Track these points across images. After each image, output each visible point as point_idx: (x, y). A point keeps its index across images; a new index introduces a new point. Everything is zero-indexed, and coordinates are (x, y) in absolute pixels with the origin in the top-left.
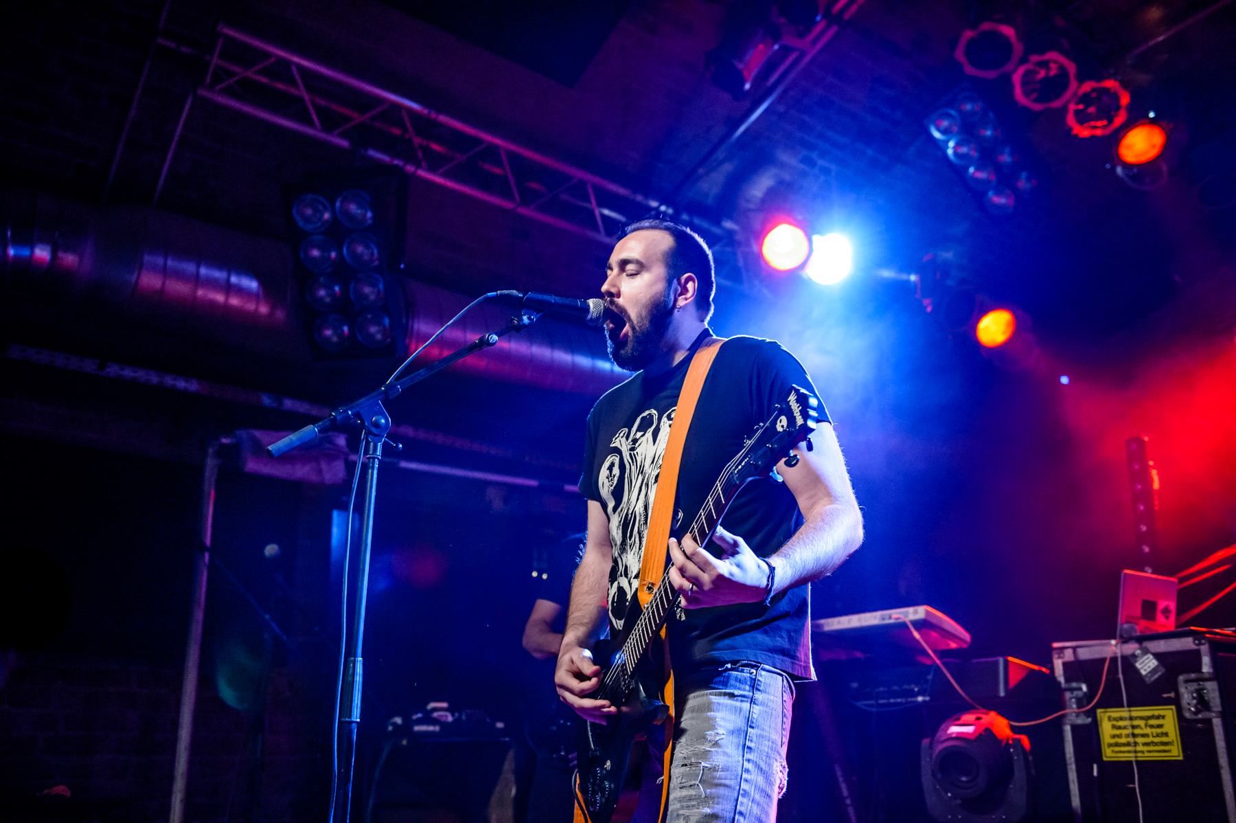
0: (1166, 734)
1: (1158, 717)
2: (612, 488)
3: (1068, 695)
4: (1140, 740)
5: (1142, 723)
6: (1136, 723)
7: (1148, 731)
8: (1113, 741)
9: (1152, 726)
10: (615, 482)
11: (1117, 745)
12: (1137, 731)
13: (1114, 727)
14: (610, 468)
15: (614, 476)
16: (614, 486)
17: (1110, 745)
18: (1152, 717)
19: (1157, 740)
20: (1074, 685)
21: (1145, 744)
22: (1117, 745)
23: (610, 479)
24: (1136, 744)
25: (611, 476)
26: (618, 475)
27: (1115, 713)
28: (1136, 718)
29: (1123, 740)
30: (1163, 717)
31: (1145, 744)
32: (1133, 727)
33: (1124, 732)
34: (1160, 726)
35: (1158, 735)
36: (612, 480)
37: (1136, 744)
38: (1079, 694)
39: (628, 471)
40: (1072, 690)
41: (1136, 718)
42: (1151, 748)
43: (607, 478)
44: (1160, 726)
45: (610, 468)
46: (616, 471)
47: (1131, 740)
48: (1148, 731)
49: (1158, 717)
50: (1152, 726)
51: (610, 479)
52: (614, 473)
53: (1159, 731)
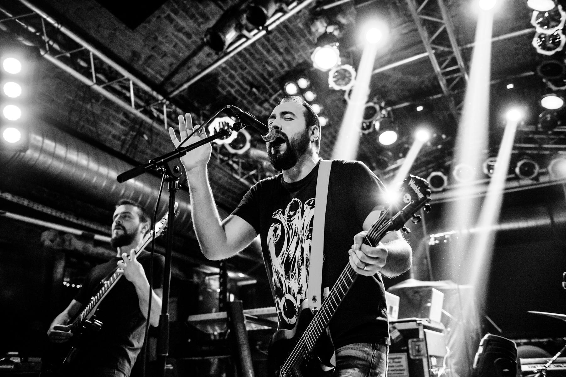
0: (402, 366)
1: (399, 358)
2: (276, 242)
9: (396, 362)
10: (278, 239)
14: (276, 230)
15: (278, 235)
16: (277, 241)
19: (398, 368)
23: (275, 236)
25: (275, 235)
26: (280, 234)
34: (399, 362)
35: (398, 366)
36: (276, 237)
39: (286, 233)
43: (273, 236)
45: (276, 230)
46: (279, 232)
50: (396, 362)
51: (275, 236)
52: (277, 233)
53: (399, 364)
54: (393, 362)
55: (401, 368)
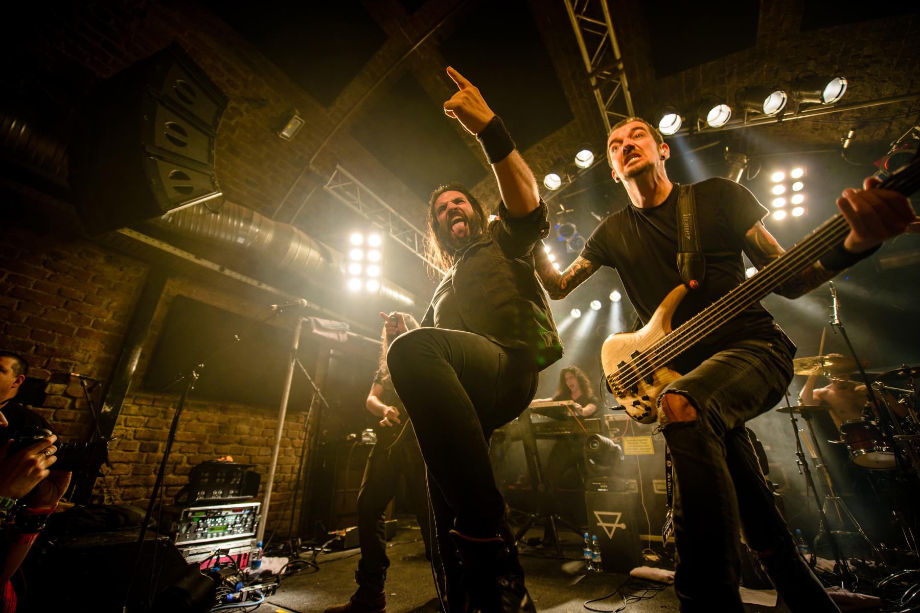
0: (648, 446)
1: (645, 440)
3: (610, 432)
4: (638, 448)
5: (639, 442)
6: (637, 442)
7: (641, 445)
8: (628, 448)
11: (630, 449)
12: (637, 445)
13: (629, 443)
17: (627, 449)
18: (643, 440)
19: (644, 448)
20: (613, 429)
21: (641, 449)
22: (630, 449)
24: (637, 449)
27: (629, 438)
28: (637, 440)
29: (631, 448)
30: (647, 440)
31: (641, 449)
32: (636, 443)
33: (632, 445)
34: (646, 443)
35: (645, 446)
37: (637, 449)
38: (615, 432)
40: (612, 431)
41: (637, 440)
42: (643, 450)
44: (646, 443)
47: (635, 447)
48: (641, 445)
49: (645, 440)
53: (646, 444)
54: (641, 443)
55: (648, 447)
